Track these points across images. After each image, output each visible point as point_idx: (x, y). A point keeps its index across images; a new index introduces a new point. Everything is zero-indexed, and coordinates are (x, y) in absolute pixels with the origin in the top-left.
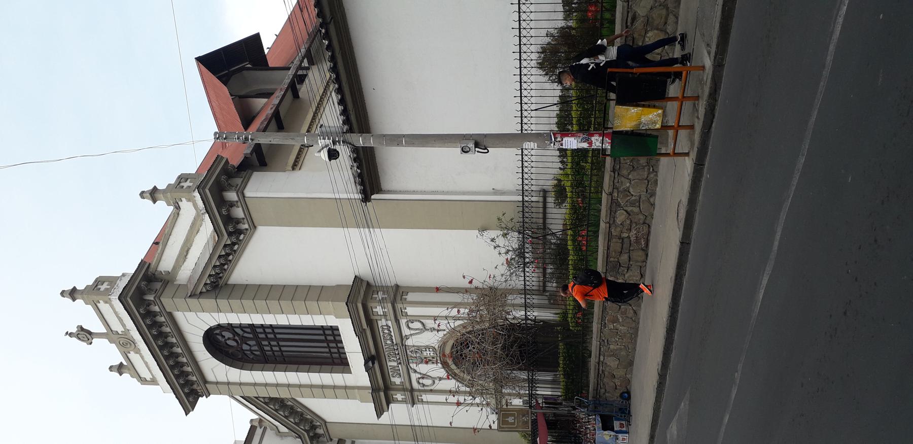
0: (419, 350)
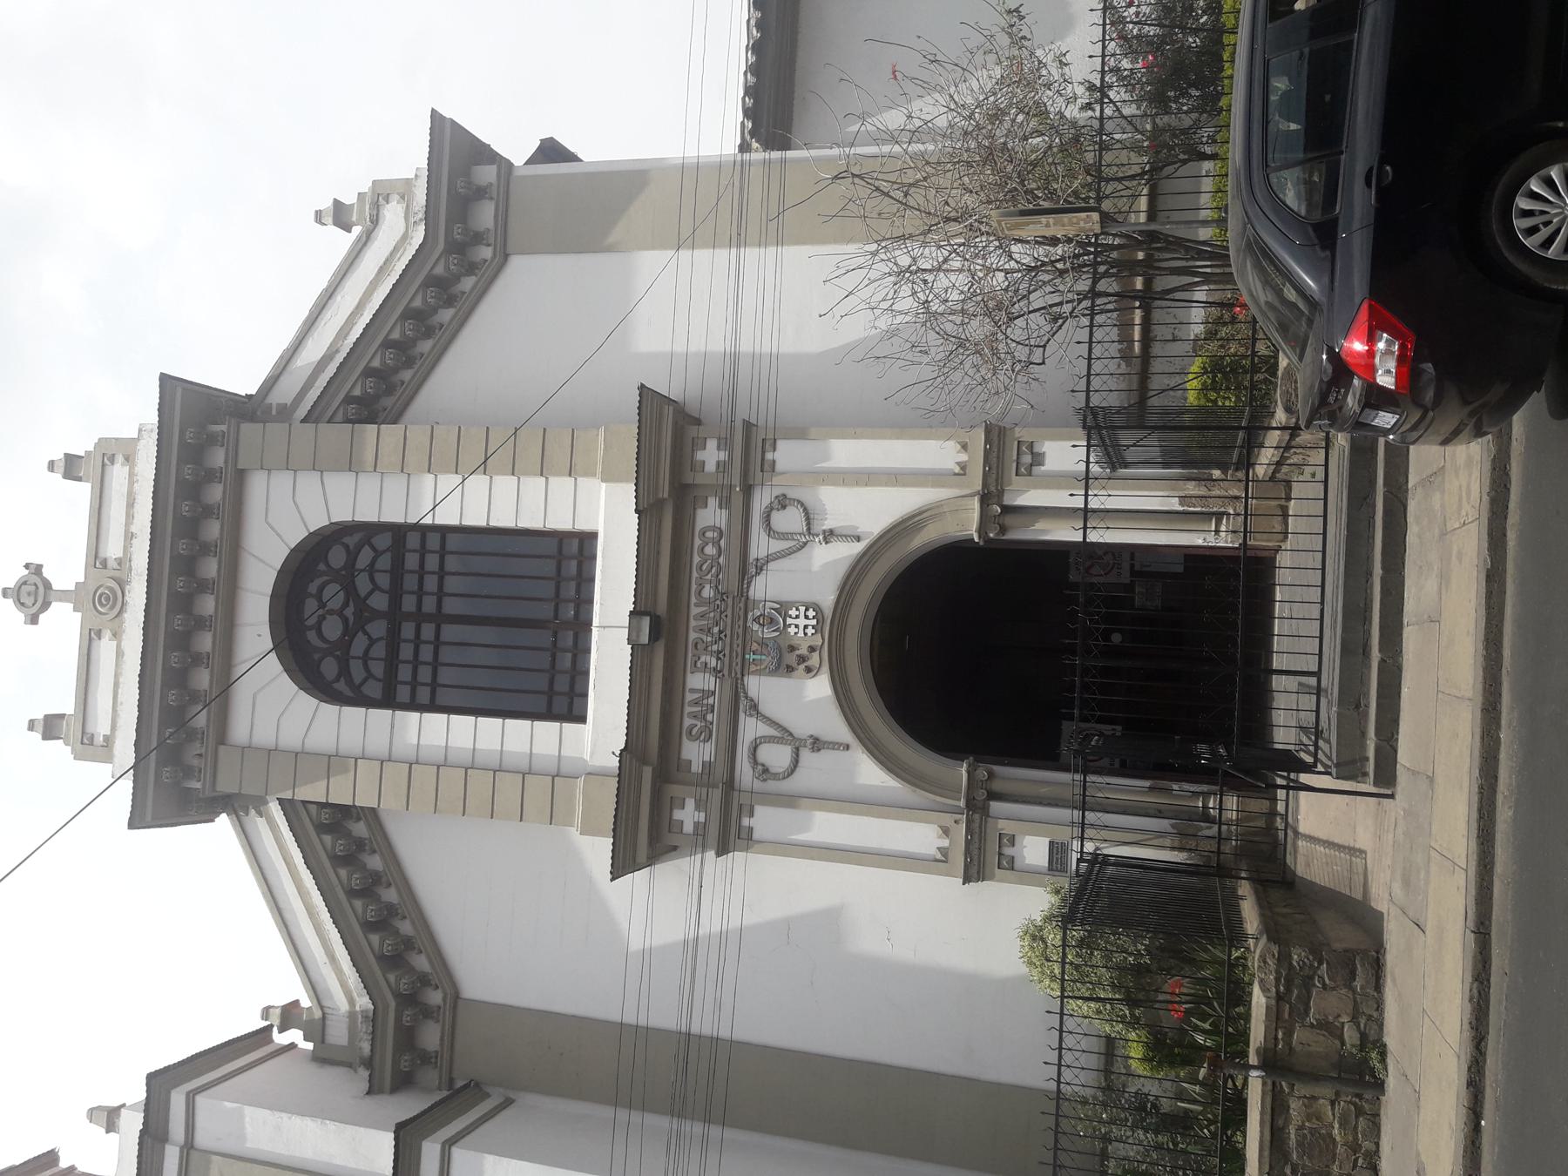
0: (780, 615)
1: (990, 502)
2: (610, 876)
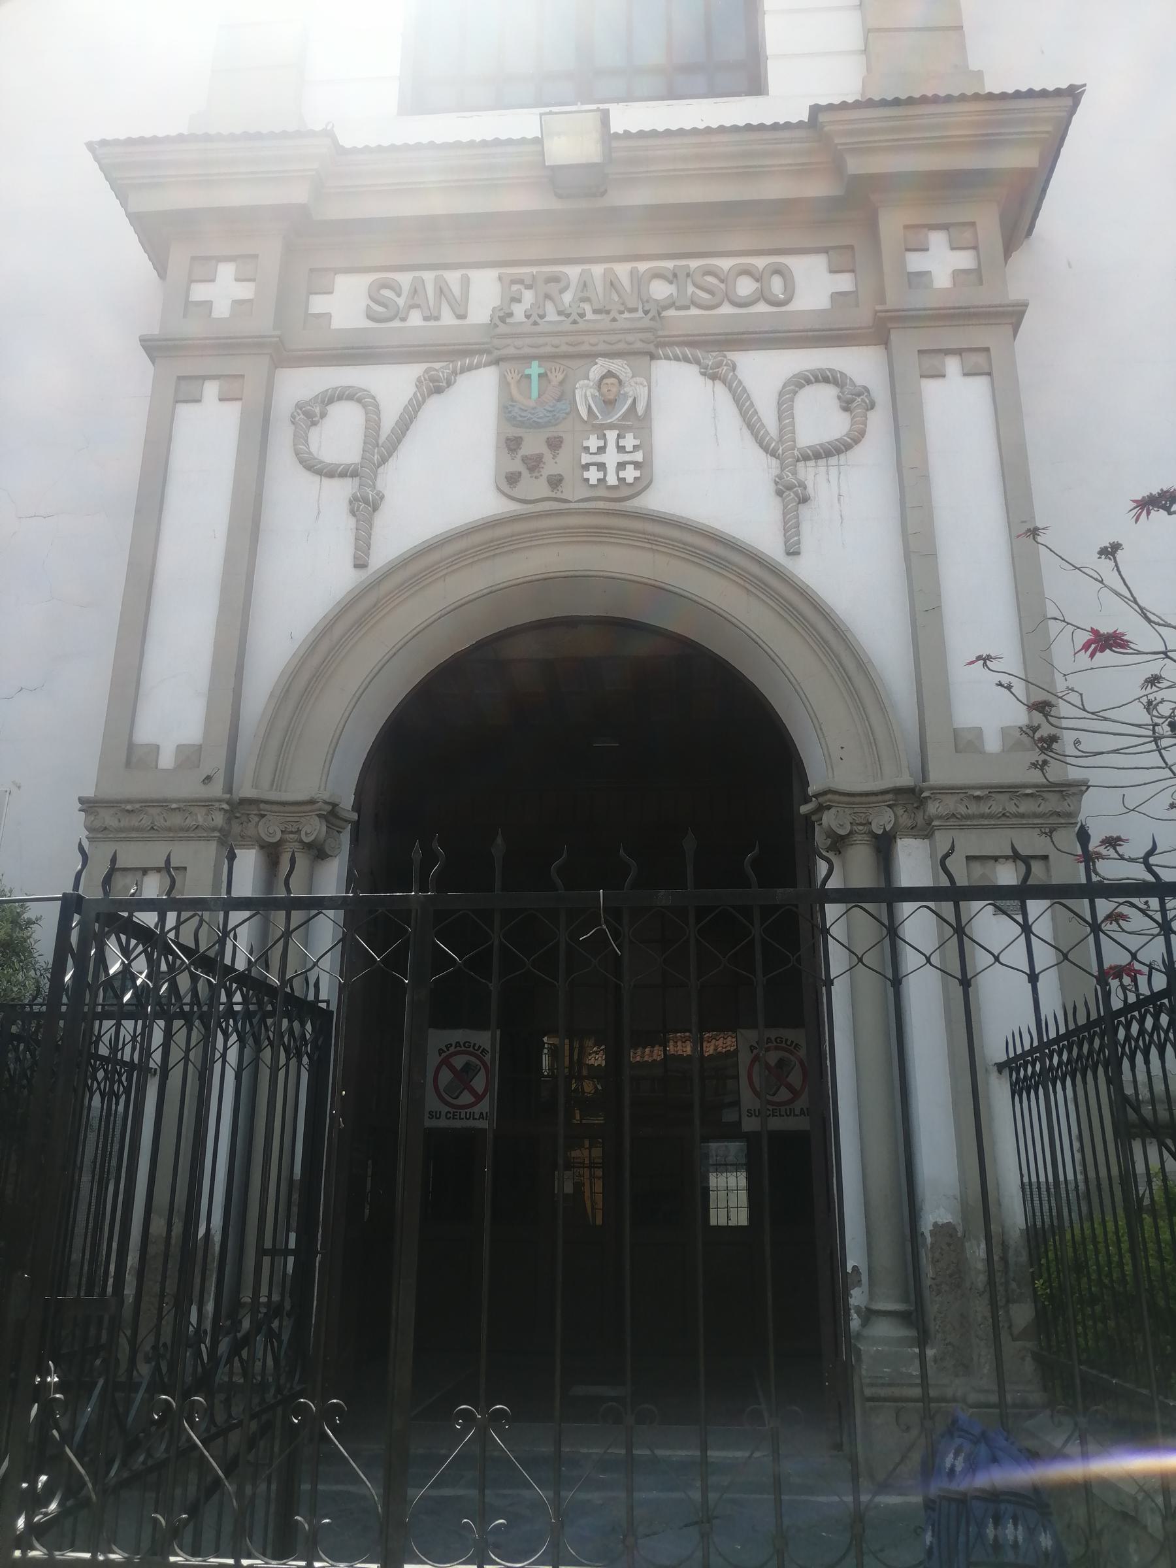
0: (624, 417)
1: (900, 811)
2: (97, 138)
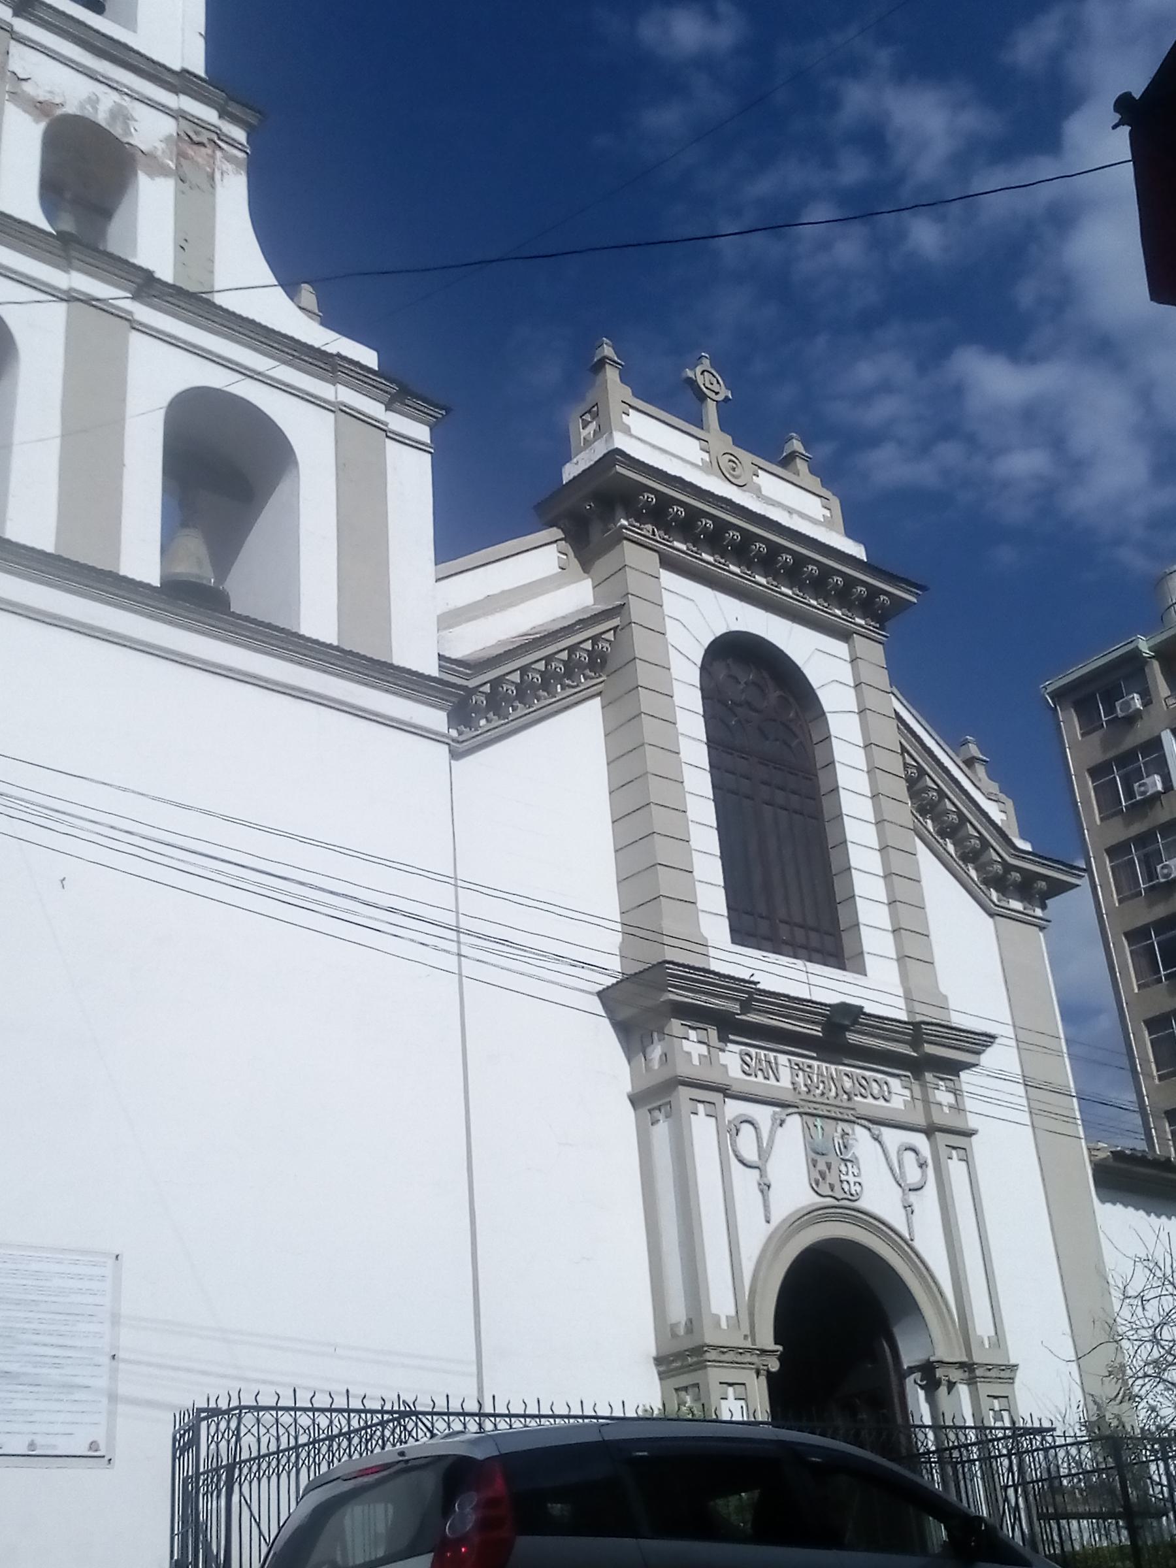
0: (851, 1157)
